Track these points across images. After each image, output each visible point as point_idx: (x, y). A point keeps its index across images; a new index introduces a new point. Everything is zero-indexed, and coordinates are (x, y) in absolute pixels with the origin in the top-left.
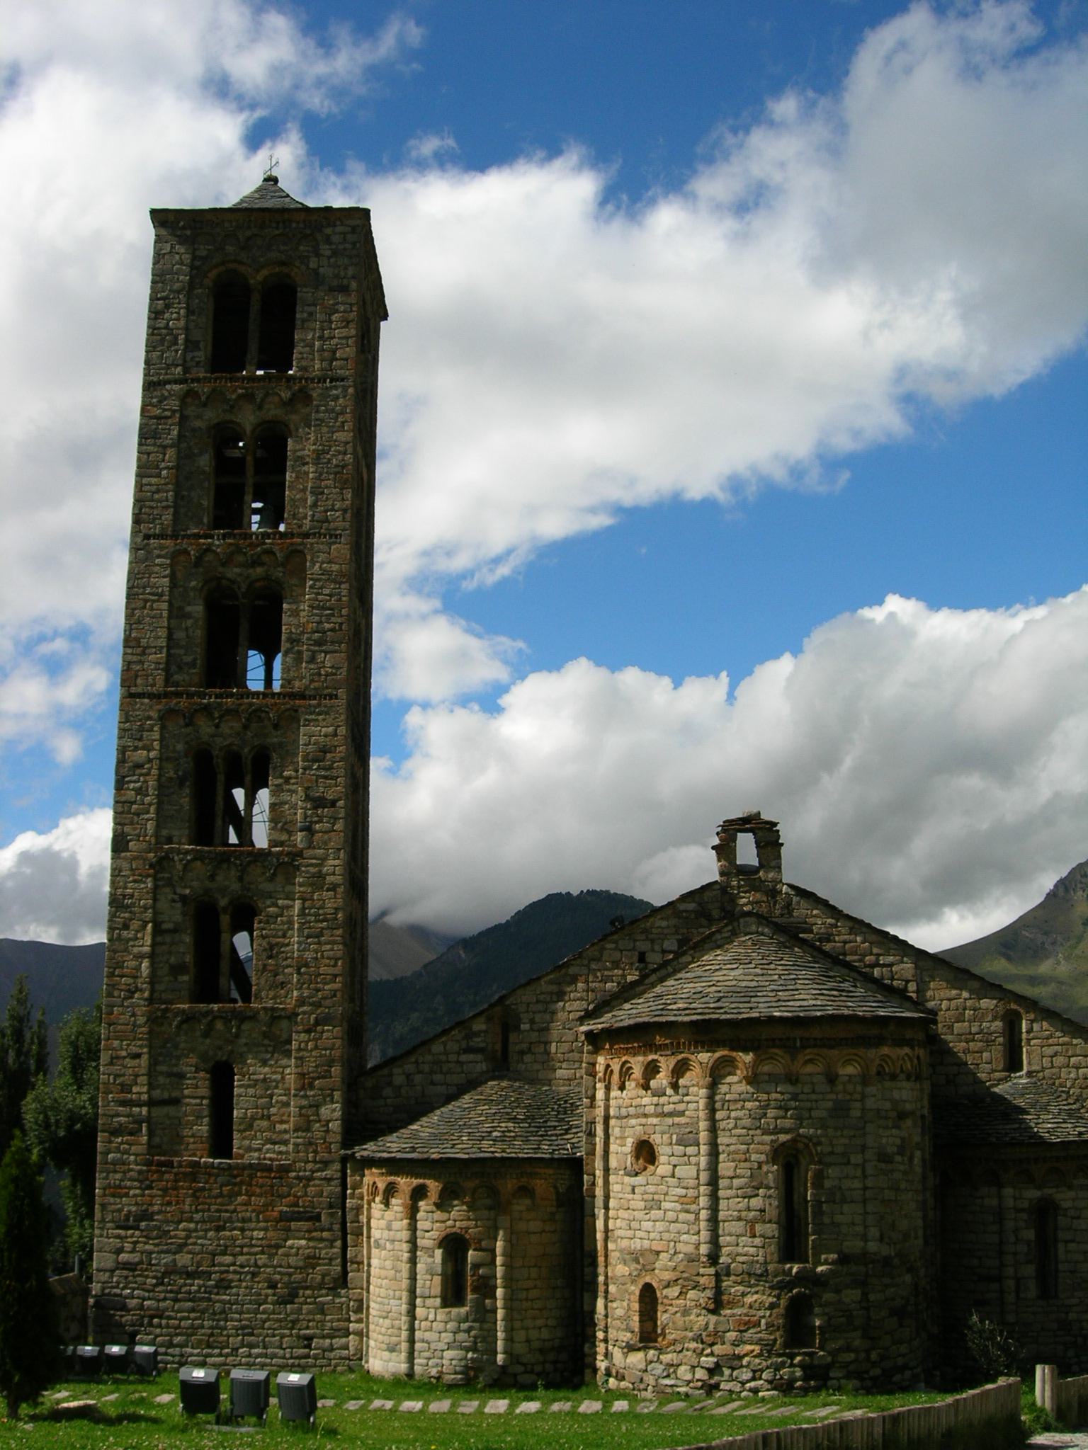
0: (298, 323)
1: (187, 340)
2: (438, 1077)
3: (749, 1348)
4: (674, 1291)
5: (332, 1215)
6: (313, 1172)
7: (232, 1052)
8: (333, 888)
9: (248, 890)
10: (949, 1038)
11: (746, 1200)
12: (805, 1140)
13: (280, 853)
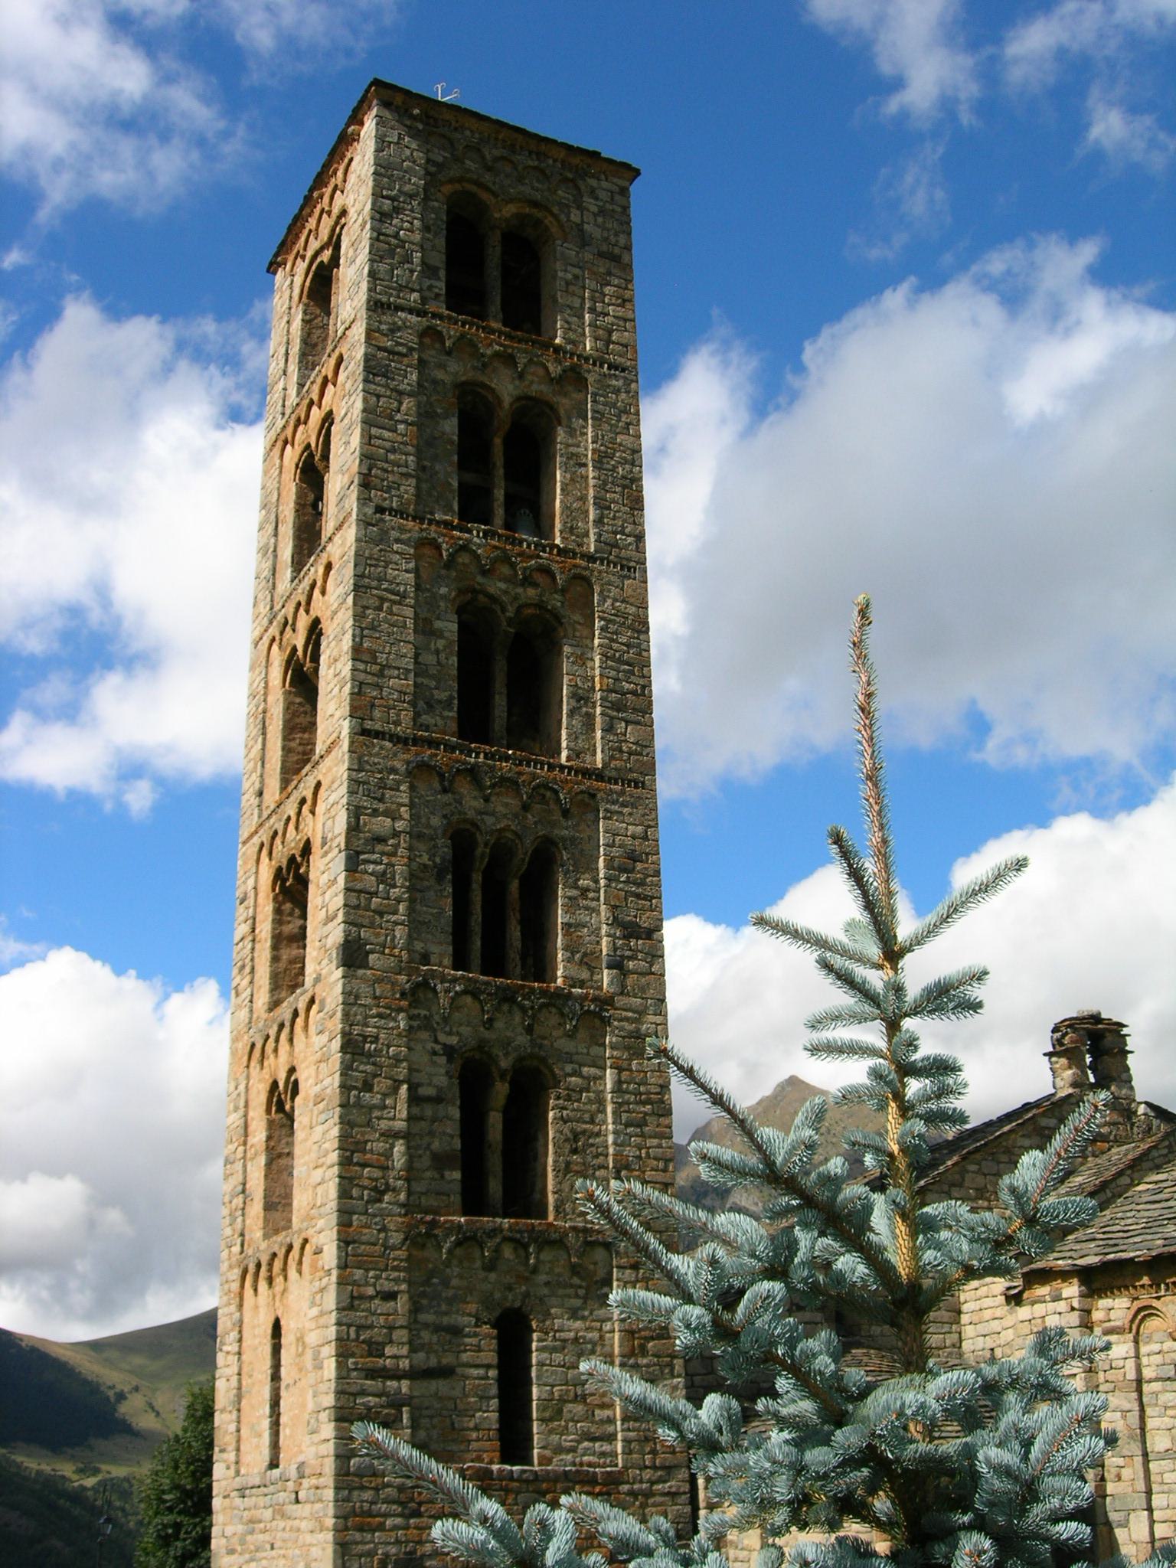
6: (652, 1483)
7: (527, 1295)
9: (541, 1046)
13: (585, 997)
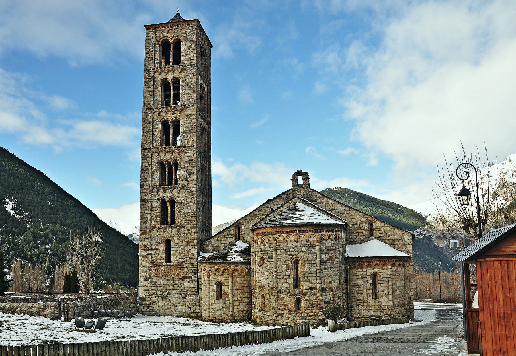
0: (182, 51)
1: (155, 58)
2: (222, 242)
3: (286, 311)
4: (268, 296)
5: (195, 277)
8: (193, 195)
10: (354, 229)
11: (285, 273)
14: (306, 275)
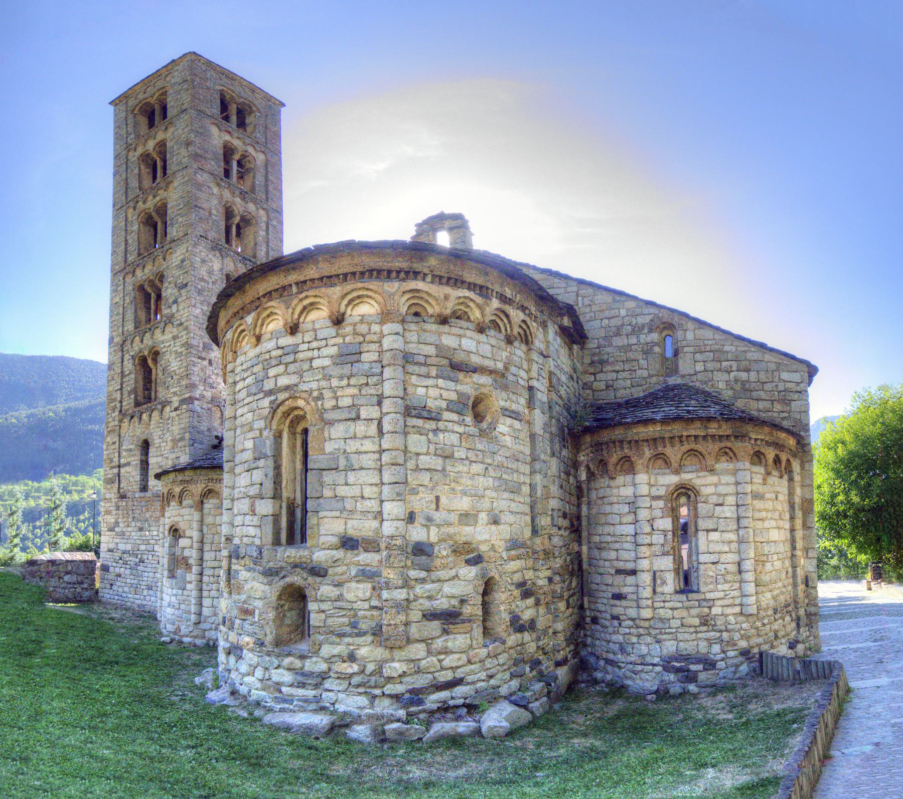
12: (305, 395)
14: (328, 477)
